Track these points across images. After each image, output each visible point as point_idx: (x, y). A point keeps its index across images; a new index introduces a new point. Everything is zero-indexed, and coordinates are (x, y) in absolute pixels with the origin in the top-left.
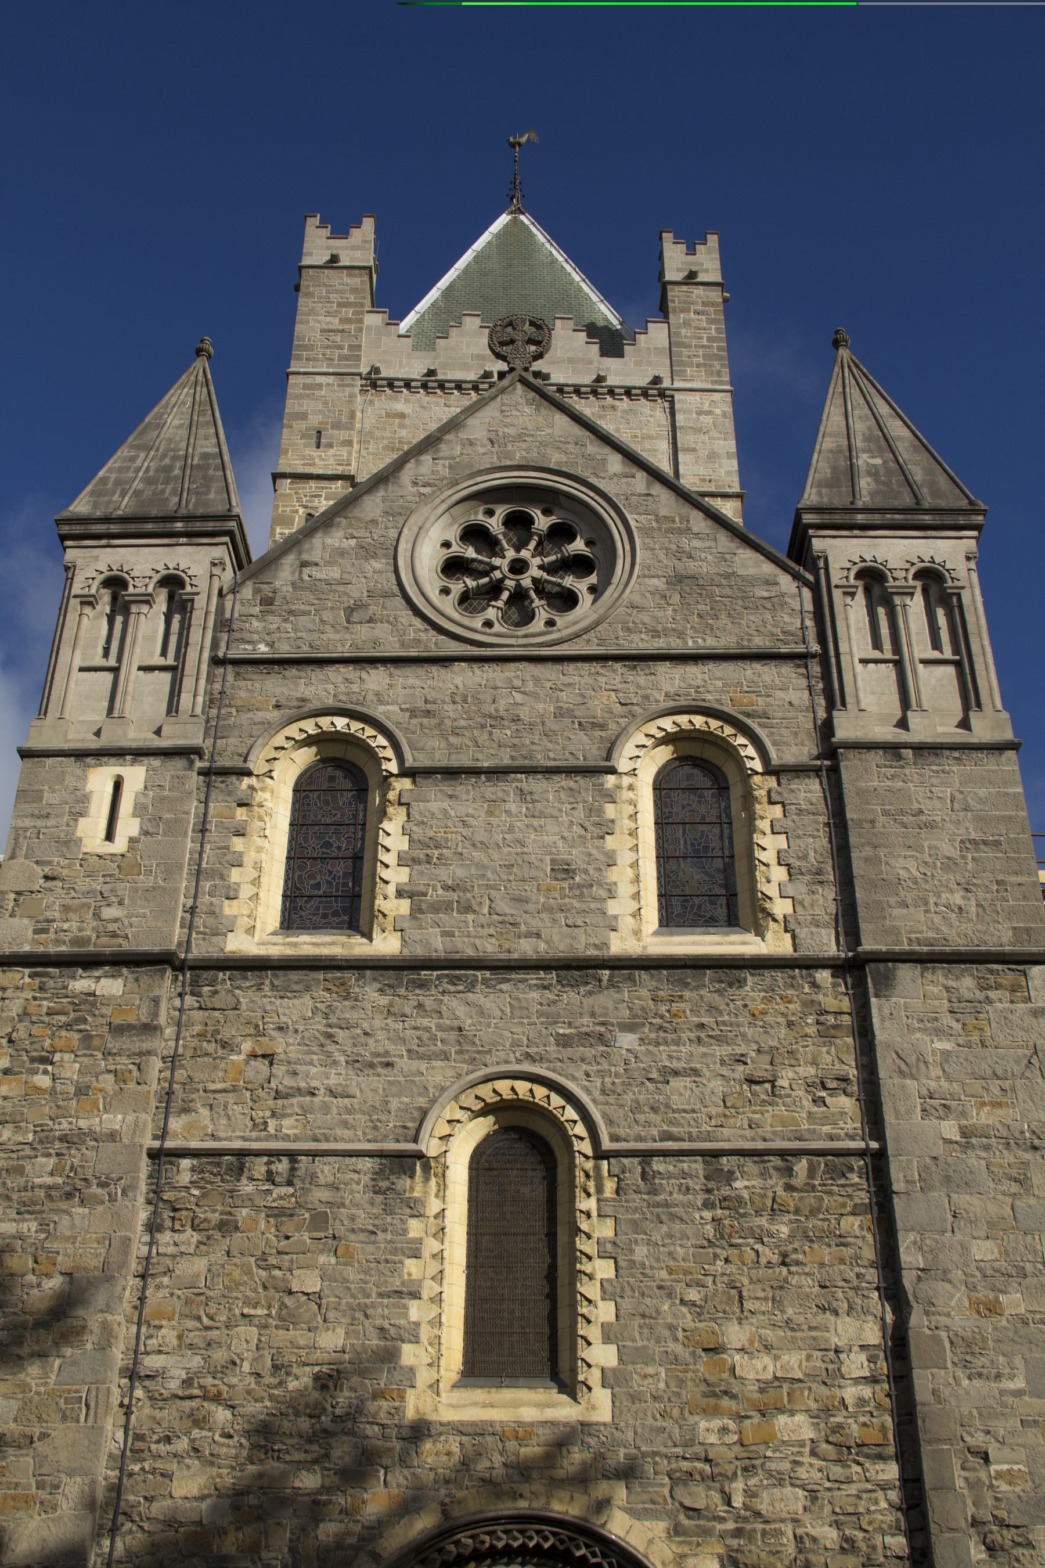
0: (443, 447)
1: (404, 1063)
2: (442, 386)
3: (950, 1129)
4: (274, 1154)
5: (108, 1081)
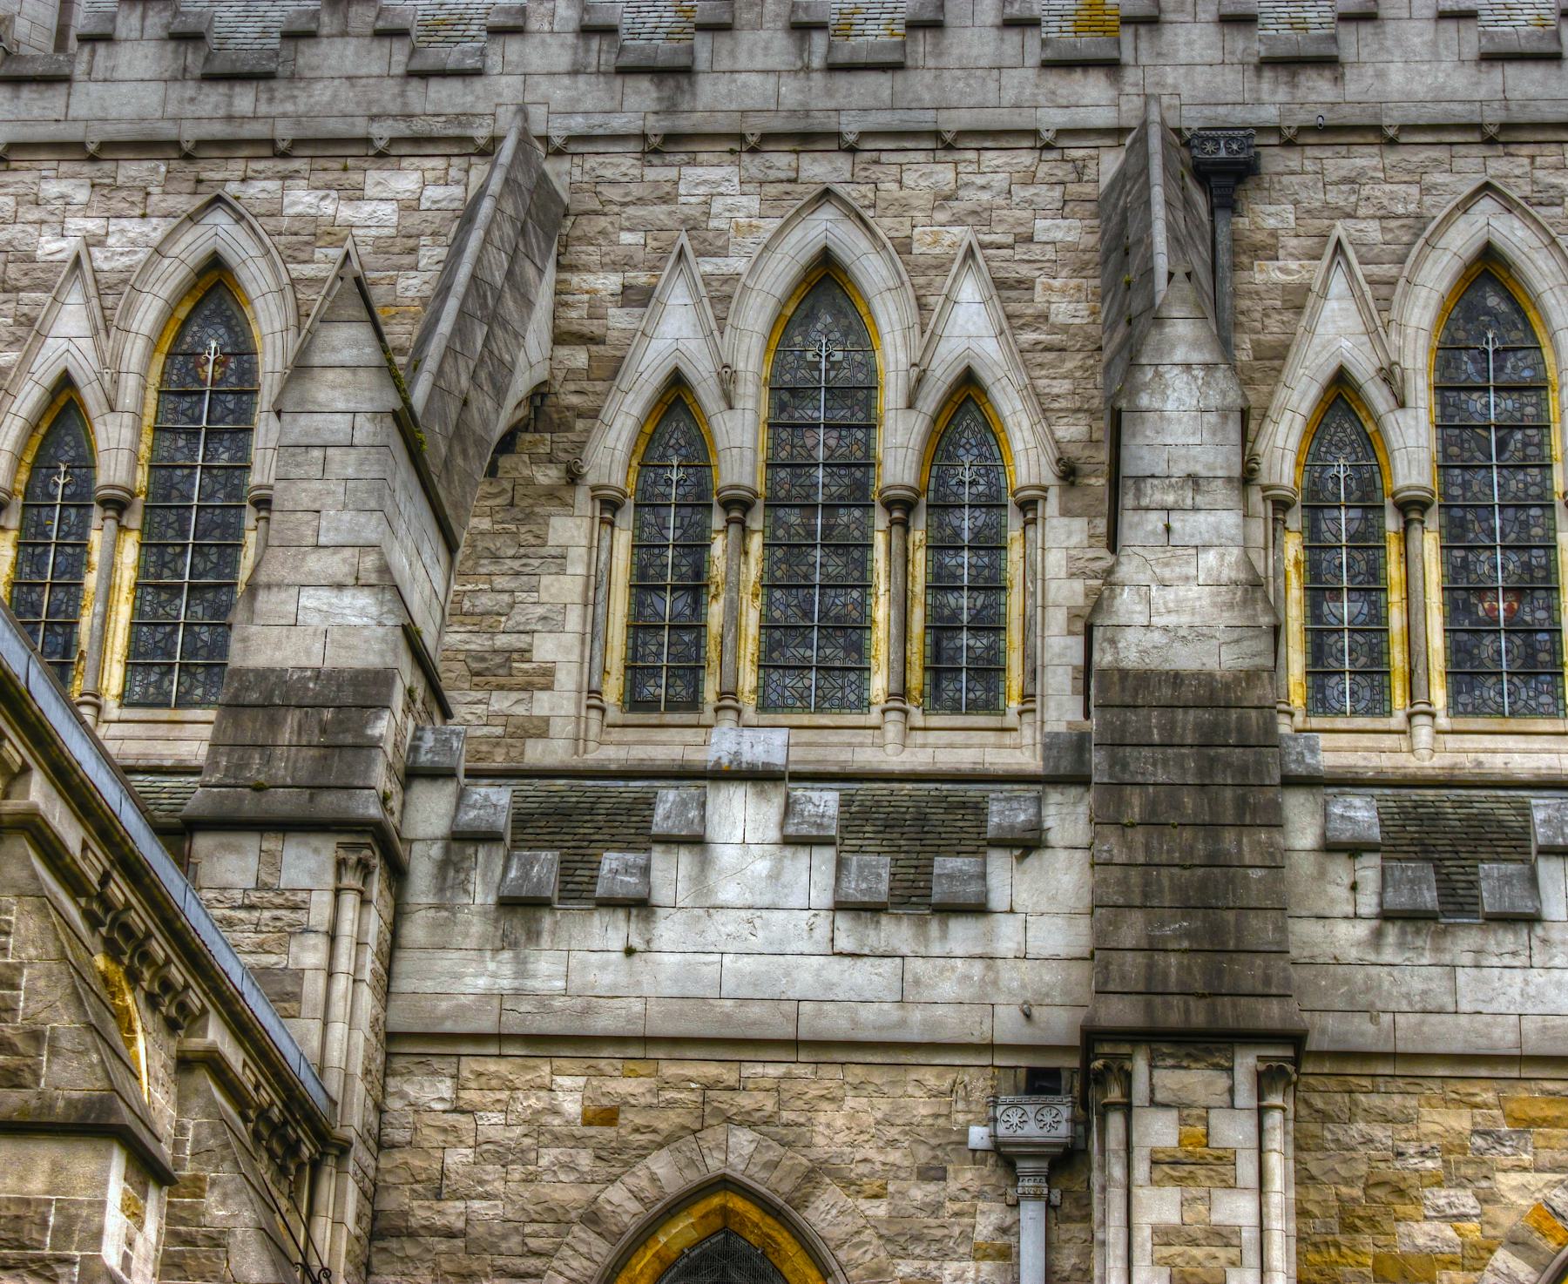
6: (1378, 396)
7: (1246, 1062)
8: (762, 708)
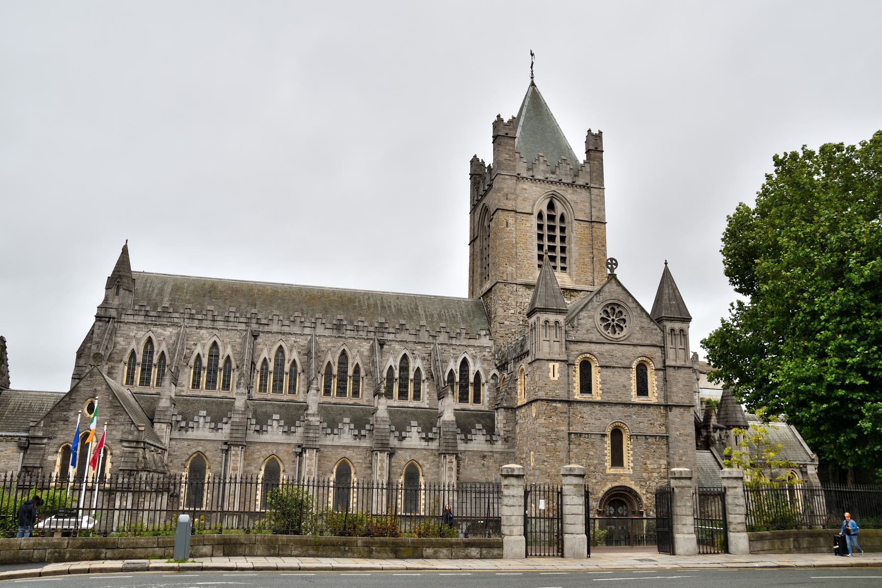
1: (603, 419)
2: (535, 180)
3: (678, 433)
4: (586, 434)
6: (268, 361)
7: (240, 447)
8: (206, 389)
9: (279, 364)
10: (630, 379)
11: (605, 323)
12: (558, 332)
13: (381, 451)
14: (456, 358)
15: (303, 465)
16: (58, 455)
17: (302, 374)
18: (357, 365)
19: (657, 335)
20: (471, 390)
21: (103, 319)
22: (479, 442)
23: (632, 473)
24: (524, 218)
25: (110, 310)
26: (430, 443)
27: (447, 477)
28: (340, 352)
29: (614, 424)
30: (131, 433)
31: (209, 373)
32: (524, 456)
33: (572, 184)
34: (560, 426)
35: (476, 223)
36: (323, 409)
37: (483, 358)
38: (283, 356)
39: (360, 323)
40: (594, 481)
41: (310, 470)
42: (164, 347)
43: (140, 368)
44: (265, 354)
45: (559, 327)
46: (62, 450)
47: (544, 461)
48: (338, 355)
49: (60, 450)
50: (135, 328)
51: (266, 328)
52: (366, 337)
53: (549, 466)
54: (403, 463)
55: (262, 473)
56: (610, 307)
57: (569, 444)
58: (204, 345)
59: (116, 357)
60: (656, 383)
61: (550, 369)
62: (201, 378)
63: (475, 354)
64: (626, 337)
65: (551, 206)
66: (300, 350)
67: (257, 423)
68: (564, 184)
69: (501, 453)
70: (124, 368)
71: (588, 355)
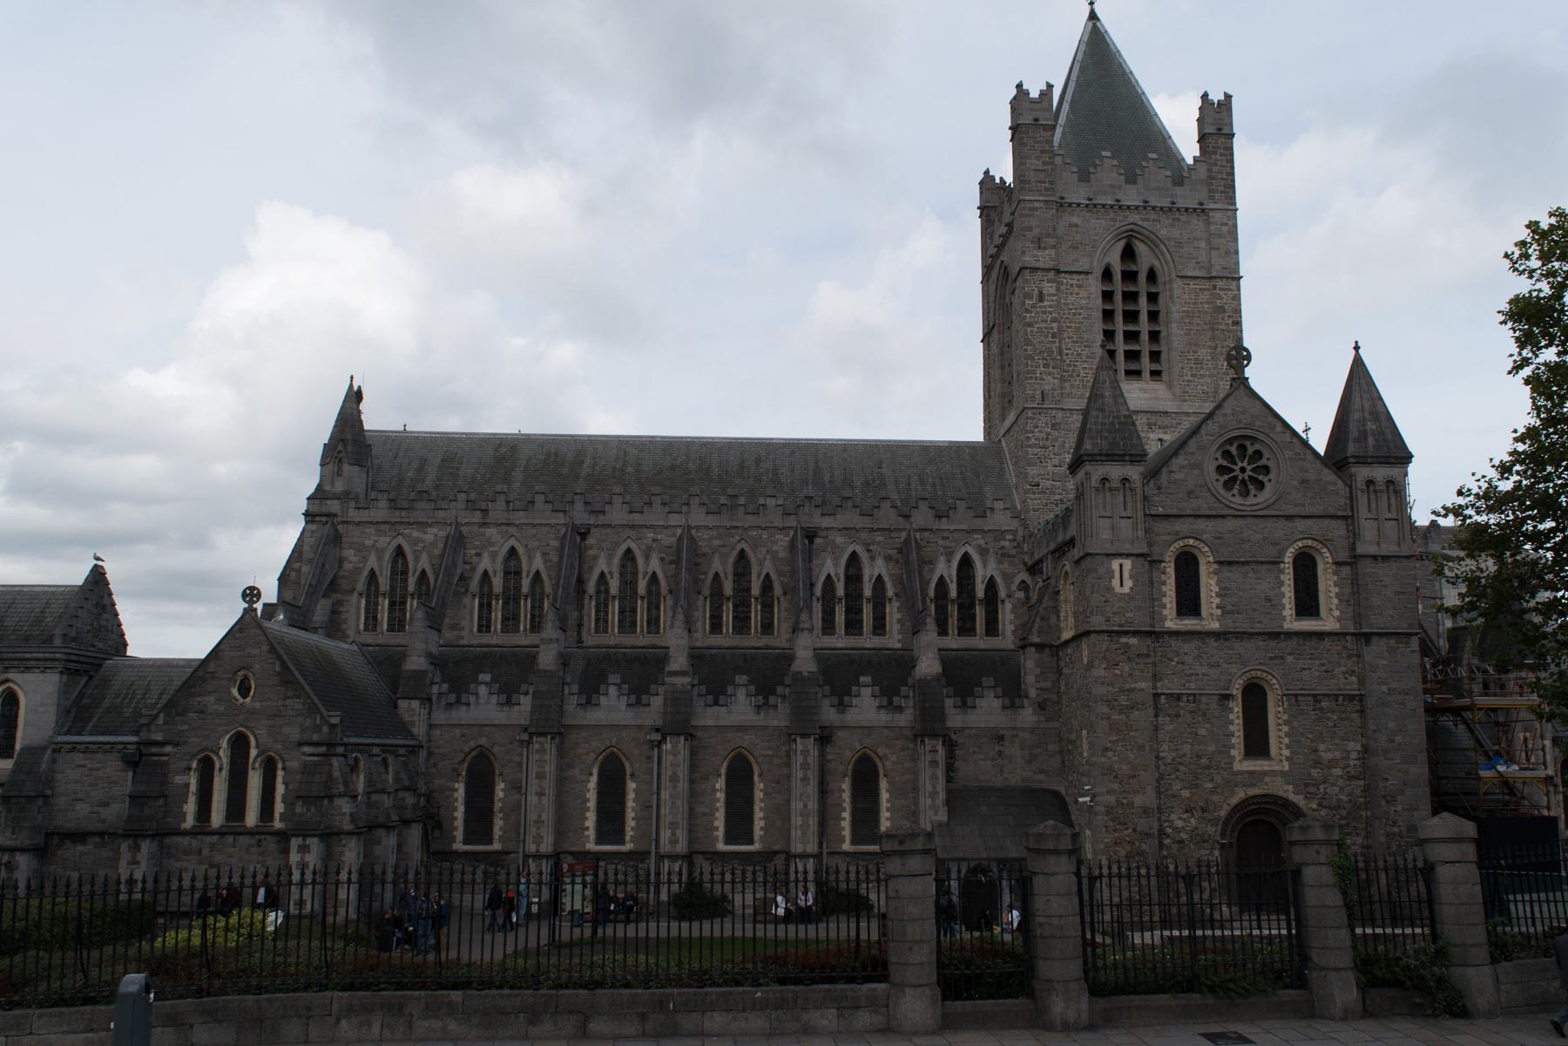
0: (1215, 417)
1: (1224, 665)
2: (1095, 206)
3: (1384, 688)
4: (1189, 695)
5: (1137, 672)
6: (608, 576)
7: (549, 737)
8: (502, 632)
9: (629, 582)
10: (1282, 583)
11: (1226, 477)
12: (1129, 499)
13: (803, 736)
14: (949, 555)
15: (664, 765)
16: (192, 773)
17: (668, 597)
18: (767, 575)
19: (1338, 493)
20: (980, 612)
21: (318, 519)
22: (988, 710)
23: (1287, 768)
24: (1075, 282)
25: (329, 502)
26: (897, 716)
27: (927, 778)
28: (735, 553)
29: (1248, 674)
30: (318, 729)
31: (506, 604)
32: (1073, 736)
33: (1171, 210)
34: (1136, 682)
35: (992, 299)
36: (697, 657)
37: (1000, 552)
38: (635, 566)
39: (769, 499)
40: (1209, 785)
41: (674, 773)
42: (425, 563)
43: (387, 602)
44: (602, 565)
45: (1131, 490)
46: (198, 765)
47: (1107, 750)
48: (731, 560)
49: (194, 765)
50: (373, 532)
51: (602, 519)
52: (781, 526)
53: (1115, 759)
54: (848, 754)
55: (594, 779)
56: (1235, 445)
57: (1156, 716)
58: (493, 556)
59: (344, 584)
60: (1337, 589)
61: (1113, 571)
62: (493, 614)
63: (984, 546)
64: (1271, 501)
65: (1129, 254)
66: (664, 555)
67: (580, 693)
68: (1154, 208)
69: (1032, 731)
70: (359, 602)
71: (1191, 542)
